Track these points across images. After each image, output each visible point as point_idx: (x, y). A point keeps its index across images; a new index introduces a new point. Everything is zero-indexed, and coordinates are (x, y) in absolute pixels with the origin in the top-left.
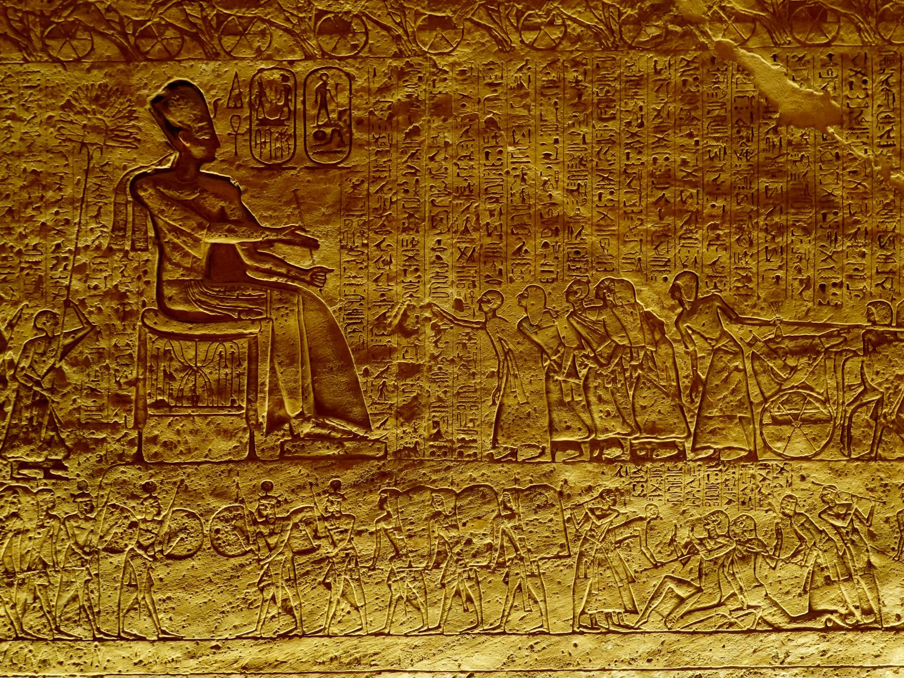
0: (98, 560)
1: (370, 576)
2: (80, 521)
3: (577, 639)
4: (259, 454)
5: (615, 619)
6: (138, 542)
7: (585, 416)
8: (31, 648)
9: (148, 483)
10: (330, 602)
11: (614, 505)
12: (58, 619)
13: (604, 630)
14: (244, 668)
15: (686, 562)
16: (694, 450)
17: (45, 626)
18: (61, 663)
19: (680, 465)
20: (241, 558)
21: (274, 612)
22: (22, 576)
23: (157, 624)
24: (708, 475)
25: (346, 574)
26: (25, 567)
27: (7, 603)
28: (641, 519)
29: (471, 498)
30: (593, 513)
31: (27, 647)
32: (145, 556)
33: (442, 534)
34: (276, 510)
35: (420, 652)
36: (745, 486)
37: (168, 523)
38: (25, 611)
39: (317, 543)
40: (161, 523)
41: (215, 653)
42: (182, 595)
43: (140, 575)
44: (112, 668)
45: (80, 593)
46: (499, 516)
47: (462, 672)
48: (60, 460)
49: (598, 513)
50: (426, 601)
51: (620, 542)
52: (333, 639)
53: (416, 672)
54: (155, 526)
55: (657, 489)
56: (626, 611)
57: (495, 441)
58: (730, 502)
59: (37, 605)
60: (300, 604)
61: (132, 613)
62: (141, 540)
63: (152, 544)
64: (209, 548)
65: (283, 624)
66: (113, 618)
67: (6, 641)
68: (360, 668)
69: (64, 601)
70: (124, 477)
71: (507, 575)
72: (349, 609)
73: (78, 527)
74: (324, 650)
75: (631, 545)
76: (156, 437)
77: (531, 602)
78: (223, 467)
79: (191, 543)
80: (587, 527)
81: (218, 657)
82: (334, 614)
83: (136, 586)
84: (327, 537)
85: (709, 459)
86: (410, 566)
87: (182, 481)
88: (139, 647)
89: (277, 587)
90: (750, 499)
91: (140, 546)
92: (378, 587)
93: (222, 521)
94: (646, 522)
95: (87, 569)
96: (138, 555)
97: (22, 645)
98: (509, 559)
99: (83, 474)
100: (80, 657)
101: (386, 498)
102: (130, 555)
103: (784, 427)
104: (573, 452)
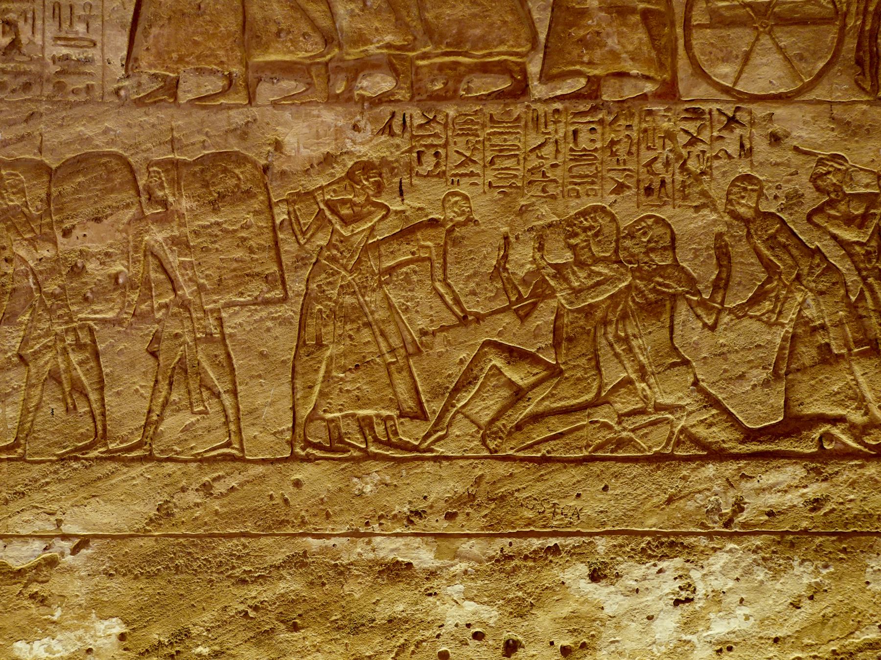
3: (304, 472)
5: (379, 430)
7: (317, 11)
11: (378, 193)
13: (356, 454)
15: (527, 315)
16: (546, 77)
19: (518, 110)
24: (575, 133)
28: (434, 223)
29: (81, 179)
30: (334, 212)
33: (22, 253)
36: (652, 155)
46: (141, 217)
47: (65, 537)
49: (345, 211)
51: (391, 270)
55: (470, 160)
56: (401, 416)
57: (130, 60)
58: (620, 188)
71: (157, 338)
75: (415, 278)
77: (206, 394)
80: (321, 240)
85: (577, 96)
90: (663, 182)
94: (442, 232)
98: (161, 307)
103: (733, 33)
104: (293, 83)
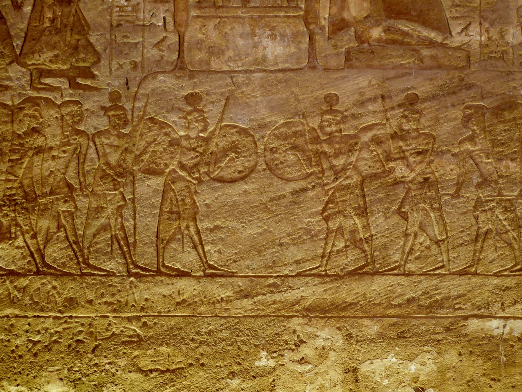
0: (133, 182)
1: (453, 205)
2: (112, 138)
4: (320, 62)
6: (180, 162)
8: (55, 283)
9: (192, 95)
10: (407, 235)
12: (86, 251)
14: (307, 309)
17: (71, 259)
18: (90, 302)
20: (302, 182)
21: (341, 244)
22: (44, 201)
23: (203, 258)
25: (425, 202)
26: (48, 190)
27: (27, 232)
31: (49, 283)
32: (189, 178)
34: (342, 126)
35: (512, 295)
37: (216, 140)
38: (47, 241)
39: (392, 164)
40: (207, 140)
41: (272, 292)
42: (233, 224)
43: (183, 200)
44: (151, 309)
45: (112, 221)
48: (89, 67)
50: (519, 237)
52: (410, 278)
53: (507, 318)
54: (200, 143)
59: (62, 234)
60: (371, 236)
61: (174, 245)
62: (185, 160)
63: (196, 165)
64: (264, 170)
65: (350, 260)
66: (152, 250)
67: (24, 275)
68: (444, 311)
69: (91, 231)
70: (164, 87)
72: (428, 243)
73: (110, 146)
74: (399, 290)
76: (202, 41)
78: (280, 75)
79: (242, 163)
81: (277, 297)
82: (412, 249)
83: (178, 213)
84: (403, 158)
86: (500, 194)
87: (232, 92)
88: (182, 284)
89: (345, 216)
91: (183, 167)
92: (463, 217)
93: (278, 138)
95: (121, 193)
96: (180, 178)
97: (44, 281)
99: (116, 83)
100: (113, 295)
101: (470, 114)
102: (170, 177)
